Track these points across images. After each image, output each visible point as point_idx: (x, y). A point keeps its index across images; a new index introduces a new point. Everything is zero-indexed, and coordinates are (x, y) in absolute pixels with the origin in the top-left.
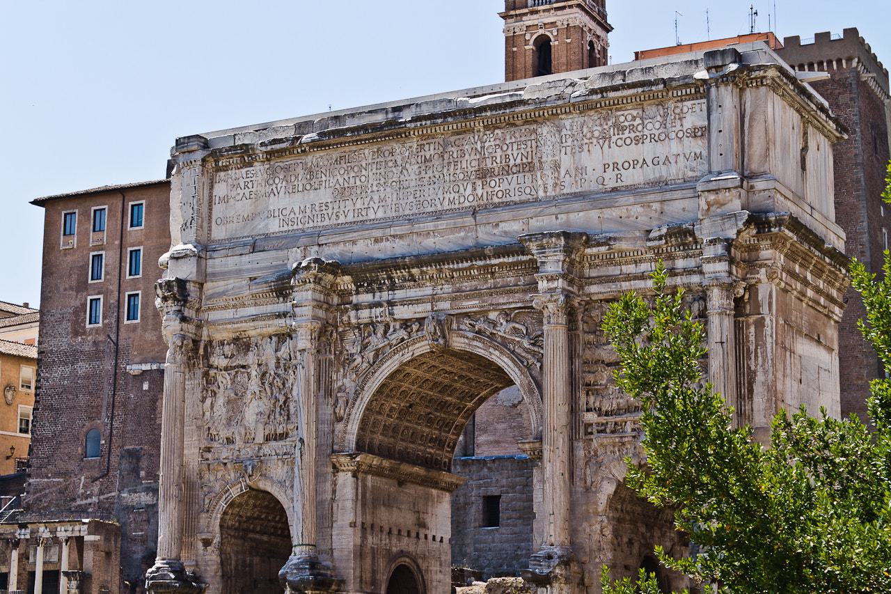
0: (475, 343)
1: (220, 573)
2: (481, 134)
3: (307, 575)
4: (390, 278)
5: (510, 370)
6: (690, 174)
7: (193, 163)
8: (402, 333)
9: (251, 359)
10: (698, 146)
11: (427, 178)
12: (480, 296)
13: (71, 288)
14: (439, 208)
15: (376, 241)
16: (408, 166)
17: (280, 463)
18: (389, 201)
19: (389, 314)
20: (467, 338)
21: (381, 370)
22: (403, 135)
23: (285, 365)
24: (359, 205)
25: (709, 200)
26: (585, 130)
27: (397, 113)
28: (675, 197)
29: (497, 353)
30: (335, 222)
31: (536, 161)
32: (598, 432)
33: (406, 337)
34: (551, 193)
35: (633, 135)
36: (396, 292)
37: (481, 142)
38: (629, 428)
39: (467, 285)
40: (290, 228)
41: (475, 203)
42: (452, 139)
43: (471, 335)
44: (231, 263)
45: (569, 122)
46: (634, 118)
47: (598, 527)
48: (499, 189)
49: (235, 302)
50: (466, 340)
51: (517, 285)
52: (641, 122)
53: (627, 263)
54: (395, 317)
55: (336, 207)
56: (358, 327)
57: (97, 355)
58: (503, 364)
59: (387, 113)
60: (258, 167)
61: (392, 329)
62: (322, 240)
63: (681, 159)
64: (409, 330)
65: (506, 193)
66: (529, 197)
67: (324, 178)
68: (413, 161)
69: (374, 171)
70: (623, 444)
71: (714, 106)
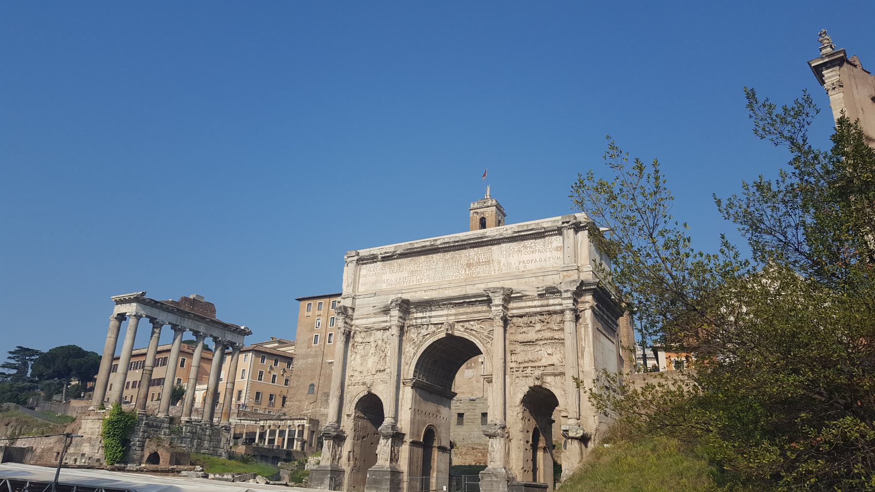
0: (464, 333)
1: (353, 430)
3: (390, 431)
6: (555, 265)
9: (372, 339)
10: (559, 254)
13: (308, 331)
14: (451, 279)
26: (511, 248)
29: (473, 337)
32: (516, 371)
35: (531, 250)
39: (462, 310)
41: (466, 277)
45: (504, 245)
46: (532, 243)
47: (516, 413)
50: (461, 332)
57: (316, 356)
59: (431, 242)
60: (379, 263)
62: (403, 291)
65: (479, 272)
69: (425, 264)
70: (527, 377)
71: (566, 237)
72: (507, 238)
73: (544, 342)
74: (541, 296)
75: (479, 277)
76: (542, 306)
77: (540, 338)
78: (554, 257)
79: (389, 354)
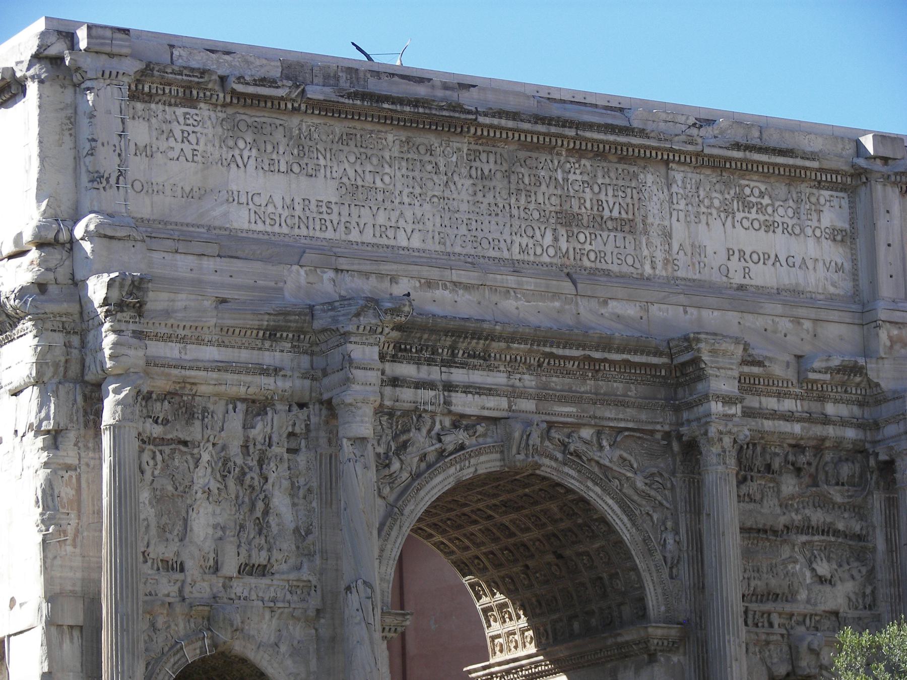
0: (566, 469)
2: (562, 159)
4: (453, 348)
5: (615, 517)
6: (832, 290)
7: (120, 76)
8: (461, 436)
9: (195, 432)
11: (484, 207)
14: (506, 254)
15: (430, 284)
16: (456, 178)
17: (267, 615)
18: (429, 225)
19: (445, 403)
20: (556, 460)
21: (429, 487)
22: (459, 130)
23: (263, 452)
24: (381, 219)
25: (891, 335)
26: (702, 193)
27: (448, 93)
28: (831, 318)
29: (598, 489)
30: (344, 237)
31: (639, 219)
33: (467, 443)
34: (660, 271)
35: (762, 218)
36: (453, 370)
37: (564, 172)
39: (557, 382)
40: (269, 229)
42: (522, 154)
43: (560, 456)
44: (184, 265)
45: (678, 175)
46: (762, 195)
48: (590, 247)
49: (187, 332)
51: (626, 395)
52: (770, 202)
53: (769, 394)
54: (453, 408)
55: (345, 211)
56: (391, 414)
58: (606, 508)
61: (438, 427)
62: (343, 264)
63: (821, 271)
64: (471, 432)
65: (600, 255)
66: (632, 270)
67: (322, 162)
68: (464, 172)
70: (768, 643)
73: (804, 538)
75: (607, 273)
76: (810, 419)
77: (796, 523)
78: (828, 260)
79: (281, 502)
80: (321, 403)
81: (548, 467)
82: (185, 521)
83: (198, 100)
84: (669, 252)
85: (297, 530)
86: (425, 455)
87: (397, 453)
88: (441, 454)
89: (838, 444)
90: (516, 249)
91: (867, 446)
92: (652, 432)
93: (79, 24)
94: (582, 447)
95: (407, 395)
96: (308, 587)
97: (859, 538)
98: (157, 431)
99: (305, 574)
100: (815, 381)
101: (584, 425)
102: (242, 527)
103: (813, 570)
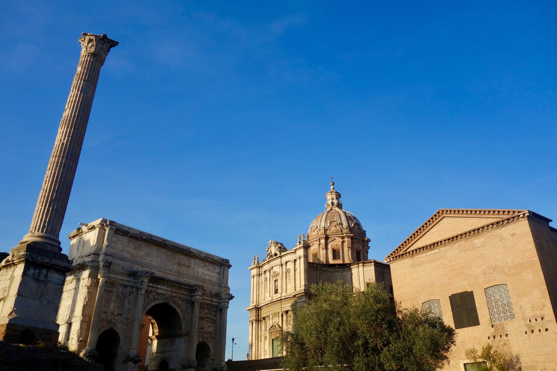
6: (216, 281)
8: (158, 296)
9: (114, 290)
10: (217, 276)
12: (177, 293)
14: (169, 268)
17: (121, 322)
20: (172, 302)
31: (190, 266)
38: (201, 332)
39: (174, 290)
42: (174, 253)
43: (172, 301)
44: (117, 262)
45: (197, 260)
46: (208, 265)
49: (116, 273)
53: (205, 296)
54: (157, 292)
60: (126, 238)
61: (154, 294)
62: (144, 265)
65: (183, 271)
70: (200, 336)
72: (200, 257)
73: (207, 320)
74: (212, 296)
75: (184, 274)
79: (126, 304)
80: (136, 288)
81: (171, 304)
82: (109, 305)
83: (125, 236)
84: (193, 272)
85: (128, 309)
86: (151, 299)
87: (147, 298)
88: (154, 299)
89: (214, 306)
90: (171, 267)
91: (218, 306)
92: (187, 300)
93: (108, 220)
94: (176, 301)
95: (150, 288)
96: (128, 319)
97: (215, 320)
98: (107, 289)
99: (128, 316)
100: (212, 295)
101: (177, 297)
102: (119, 307)
103: (208, 325)
